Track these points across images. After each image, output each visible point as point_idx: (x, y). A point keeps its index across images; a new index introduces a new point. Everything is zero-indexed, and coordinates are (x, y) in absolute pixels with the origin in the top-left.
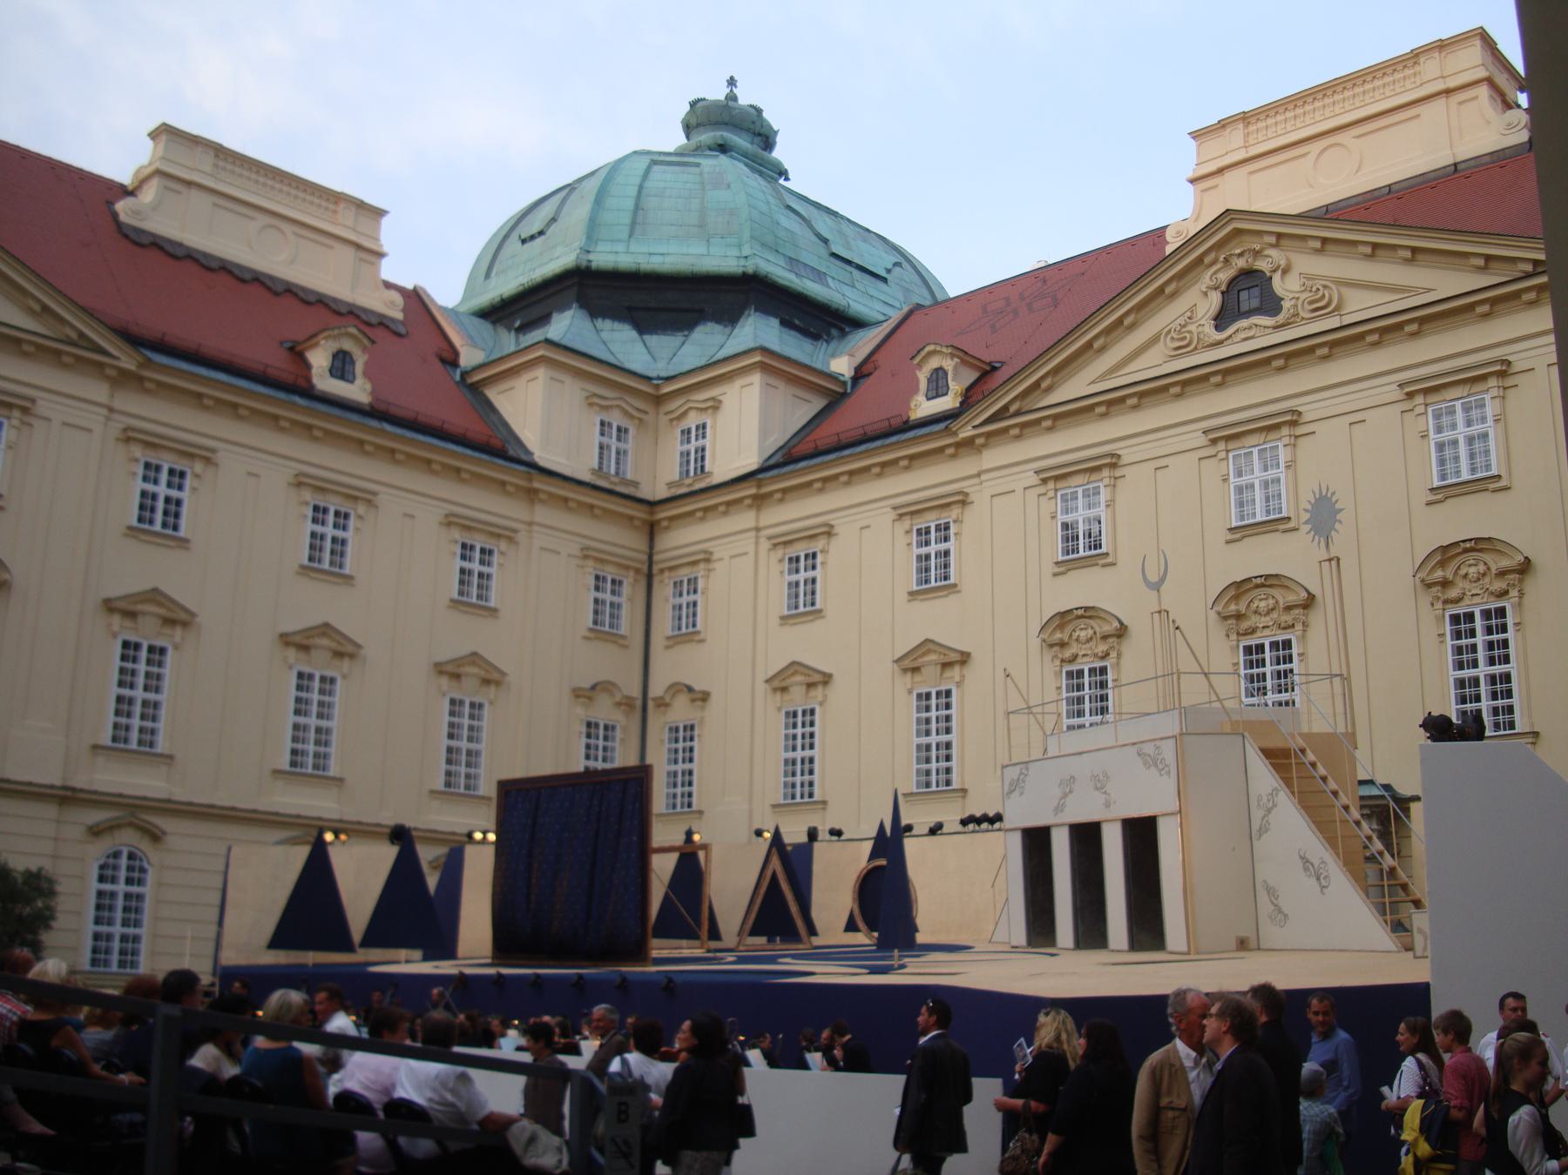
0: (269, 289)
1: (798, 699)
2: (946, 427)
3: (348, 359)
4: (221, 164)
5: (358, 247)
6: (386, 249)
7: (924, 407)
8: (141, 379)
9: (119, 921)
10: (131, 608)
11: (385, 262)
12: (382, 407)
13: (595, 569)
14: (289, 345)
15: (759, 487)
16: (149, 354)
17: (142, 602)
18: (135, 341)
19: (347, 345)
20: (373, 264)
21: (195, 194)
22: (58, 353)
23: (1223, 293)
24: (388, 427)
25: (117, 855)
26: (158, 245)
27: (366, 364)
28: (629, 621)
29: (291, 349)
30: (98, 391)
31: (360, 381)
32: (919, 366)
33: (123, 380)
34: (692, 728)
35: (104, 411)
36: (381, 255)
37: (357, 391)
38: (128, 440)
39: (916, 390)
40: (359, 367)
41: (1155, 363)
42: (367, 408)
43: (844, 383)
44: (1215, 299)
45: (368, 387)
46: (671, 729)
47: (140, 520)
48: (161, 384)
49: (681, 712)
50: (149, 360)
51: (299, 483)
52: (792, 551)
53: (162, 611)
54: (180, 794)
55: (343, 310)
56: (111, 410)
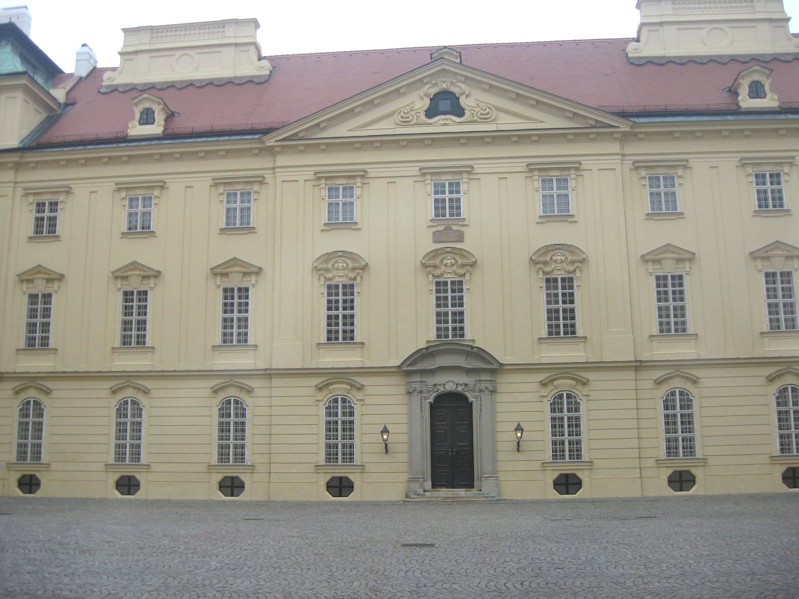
0: (720, 63)
3: (759, 85)
4: (677, 6)
5: (771, 20)
6: (789, 15)
8: (636, 134)
9: (680, 431)
10: (657, 257)
11: (790, 23)
12: (785, 106)
14: (727, 90)
16: (632, 119)
17: (662, 253)
18: (624, 115)
19: (756, 77)
20: (783, 27)
21: (665, 28)
22: (587, 134)
24: (790, 116)
25: (673, 394)
26: (650, 62)
27: (771, 85)
29: (730, 91)
30: (615, 148)
31: (769, 95)
33: (625, 137)
35: (620, 157)
36: (788, 20)
37: (769, 102)
38: (637, 168)
40: (767, 88)
42: (778, 109)
45: (776, 97)
47: (760, 206)
48: (646, 134)
50: (635, 122)
51: (743, 164)
53: (676, 256)
54: (704, 355)
55: (790, 58)
56: (623, 155)
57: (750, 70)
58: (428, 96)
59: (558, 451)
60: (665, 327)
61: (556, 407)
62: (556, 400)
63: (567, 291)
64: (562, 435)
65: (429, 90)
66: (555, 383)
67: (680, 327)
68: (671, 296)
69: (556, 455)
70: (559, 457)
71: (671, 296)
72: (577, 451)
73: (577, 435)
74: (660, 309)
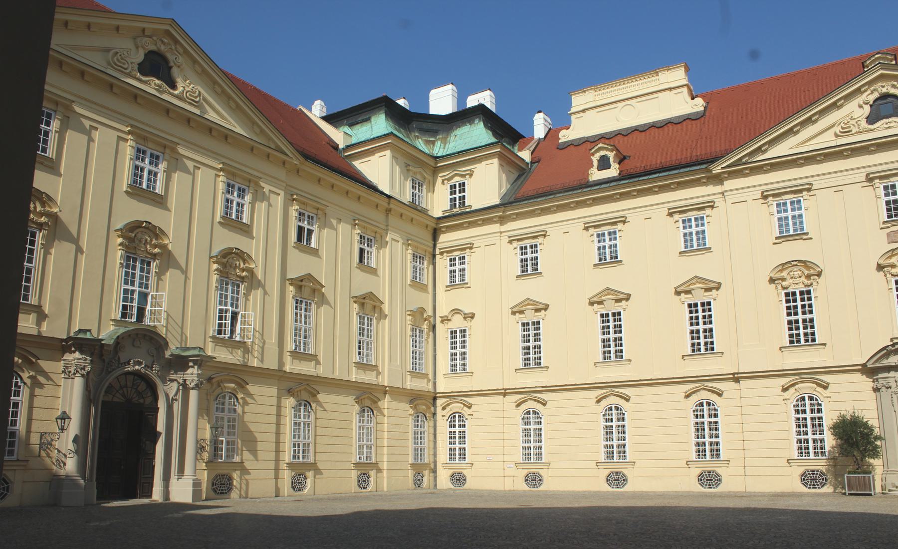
1: (530, 316)
2: (706, 168)
7: (596, 175)
13: (413, 251)
15: (504, 212)
23: (871, 106)
28: (427, 279)
32: (593, 154)
34: (465, 331)
39: (592, 166)
41: (828, 140)
43: (528, 164)
44: (867, 109)
46: (452, 332)
49: (457, 323)
52: (523, 244)
57: (596, 148)
58: (867, 104)
59: (803, 448)
60: (696, 348)
61: (800, 408)
62: (799, 402)
63: (792, 304)
64: (807, 434)
65: (868, 97)
66: (797, 387)
67: (709, 346)
68: (701, 321)
69: (802, 453)
70: (804, 454)
71: (701, 321)
72: (822, 448)
73: (820, 434)
74: (692, 332)
